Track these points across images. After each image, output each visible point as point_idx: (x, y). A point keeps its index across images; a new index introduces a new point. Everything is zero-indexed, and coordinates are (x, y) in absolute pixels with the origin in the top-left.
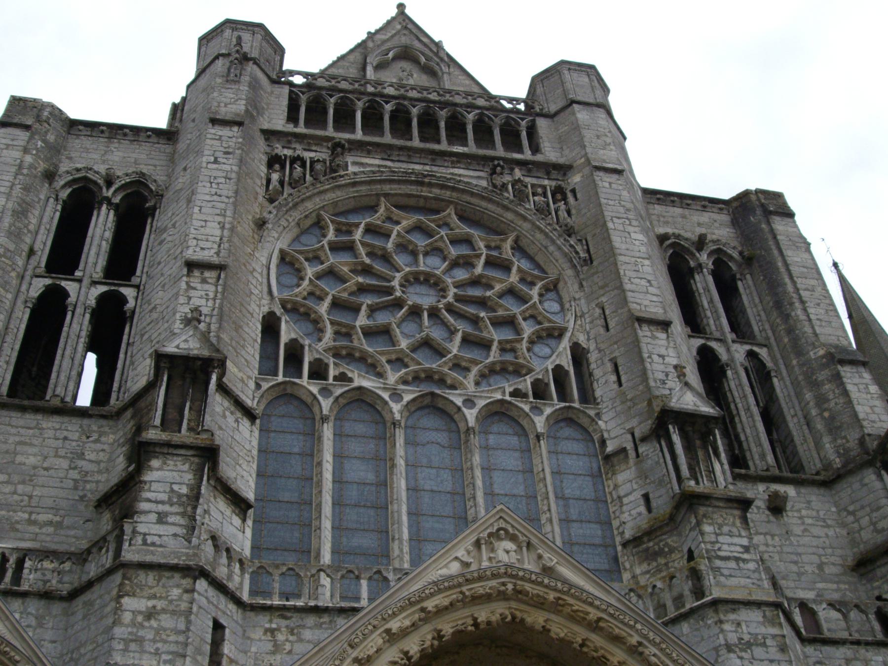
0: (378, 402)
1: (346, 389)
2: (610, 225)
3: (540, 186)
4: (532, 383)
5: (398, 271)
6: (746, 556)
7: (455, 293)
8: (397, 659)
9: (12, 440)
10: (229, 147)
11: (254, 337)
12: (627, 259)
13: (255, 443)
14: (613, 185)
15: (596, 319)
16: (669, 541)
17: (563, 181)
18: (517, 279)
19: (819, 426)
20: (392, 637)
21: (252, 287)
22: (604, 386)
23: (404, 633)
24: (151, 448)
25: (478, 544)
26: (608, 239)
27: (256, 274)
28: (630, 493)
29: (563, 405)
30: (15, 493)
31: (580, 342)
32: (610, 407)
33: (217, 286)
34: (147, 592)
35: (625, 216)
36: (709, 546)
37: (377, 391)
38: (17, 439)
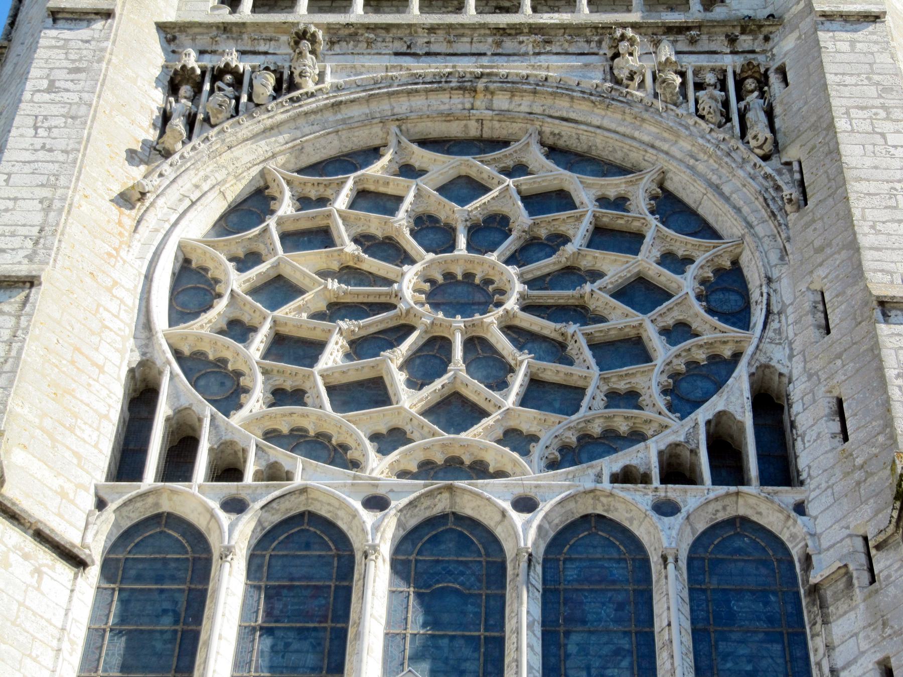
0: (341, 513)
1: (277, 493)
2: (841, 124)
3: (713, 70)
4: (661, 453)
5: (413, 262)
7: (522, 296)
10: (80, 60)
11: (104, 410)
12: (872, 187)
14: (859, 45)
15: (806, 315)
17: (764, 52)
18: (657, 254)
21: (106, 315)
22: (813, 446)
26: (834, 153)
27: (119, 292)
28: (855, 660)
29: (722, 490)
31: (773, 363)
32: (824, 485)
33: (18, 317)
35: (877, 102)
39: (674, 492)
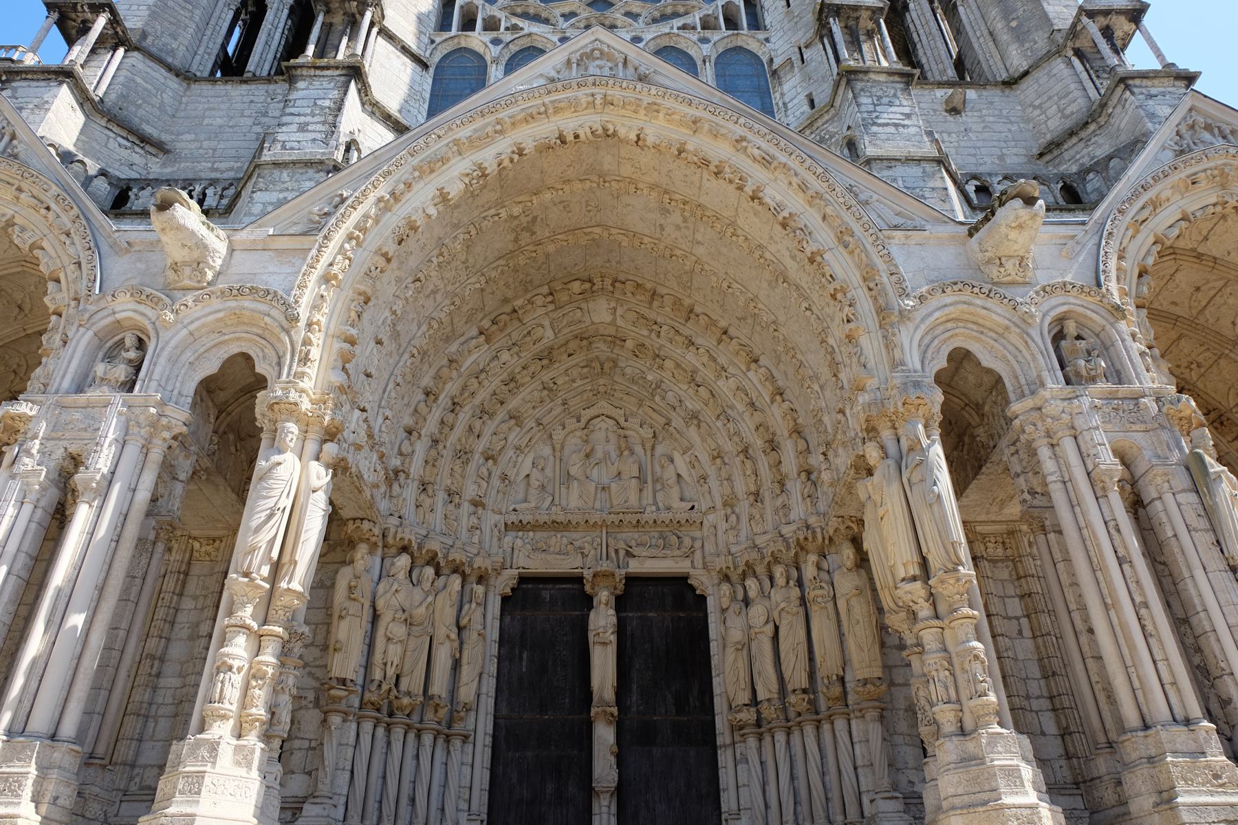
6: (906, 122)
8: (468, 171)
9: (201, 107)
13: (428, 88)
16: (830, 128)
19: (1004, 37)
20: (459, 148)
23: (475, 142)
24: (299, 72)
25: (569, 62)
29: (730, 32)
30: (201, 148)
34: (280, 186)
36: (865, 115)
37: (549, 36)
38: (206, 106)
39: (708, 34)
